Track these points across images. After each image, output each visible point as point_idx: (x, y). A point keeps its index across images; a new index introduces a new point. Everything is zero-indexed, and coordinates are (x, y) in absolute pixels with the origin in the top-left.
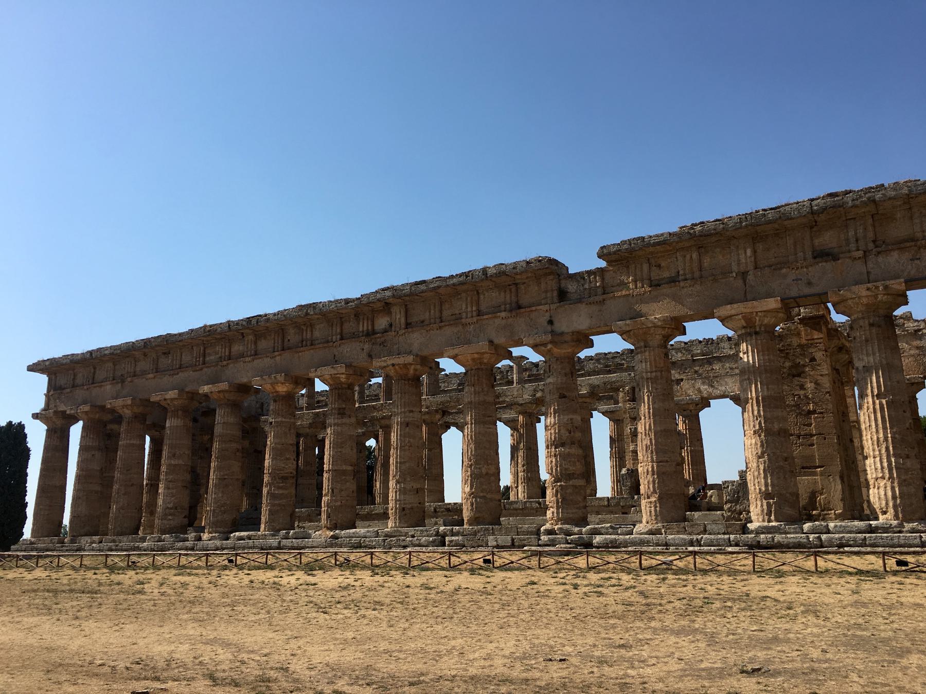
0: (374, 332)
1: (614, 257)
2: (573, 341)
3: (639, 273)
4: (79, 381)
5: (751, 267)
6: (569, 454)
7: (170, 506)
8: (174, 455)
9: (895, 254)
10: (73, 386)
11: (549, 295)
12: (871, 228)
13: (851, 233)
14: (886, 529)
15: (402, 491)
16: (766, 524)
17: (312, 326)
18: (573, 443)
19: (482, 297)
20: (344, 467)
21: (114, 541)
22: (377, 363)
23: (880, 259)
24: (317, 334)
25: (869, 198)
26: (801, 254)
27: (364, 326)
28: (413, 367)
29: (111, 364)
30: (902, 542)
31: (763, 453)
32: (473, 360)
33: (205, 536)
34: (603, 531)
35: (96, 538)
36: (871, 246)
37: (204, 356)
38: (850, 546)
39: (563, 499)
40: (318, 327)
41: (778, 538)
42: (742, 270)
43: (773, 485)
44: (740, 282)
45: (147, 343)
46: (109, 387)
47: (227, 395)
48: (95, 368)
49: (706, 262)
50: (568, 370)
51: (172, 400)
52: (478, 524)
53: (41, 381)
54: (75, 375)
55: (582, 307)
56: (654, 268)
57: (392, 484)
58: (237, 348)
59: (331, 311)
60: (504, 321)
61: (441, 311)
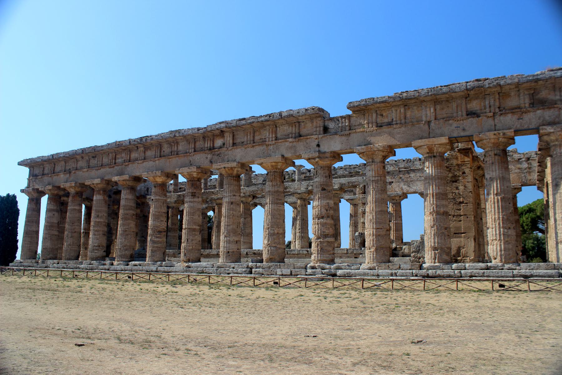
0: (214, 148)
1: (356, 109)
2: (331, 157)
3: (370, 119)
4: (46, 171)
5: (433, 118)
6: (326, 223)
7: (96, 245)
8: (98, 216)
9: (510, 116)
10: (43, 175)
11: (318, 129)
12: (498, 100)
13: (487, 103)
14: (495, 268)
15: (229, 242)
16: (433, 264)
17: (177, 143)
18: (328, 217)
19: (278, 129)
20: (194, 227)
21: (65, 263)
22: (215, 166)
23: (502, 118)
24: (180, 148)
25: (497, 83)
26: (460, 113)
27: (208, 144)
28: (236, 169)
29: (63, 163)
30: (503, 274)
31: (434, 225)
32: (272, 166)
33: (115, 263)
34: (343, 267)
35: (56, 261)
36: (497, 110)
37: (115, 159)
38: (476, 276)
39: (321, 249)
40: (181, 144)
41: (439, 272)
42: (428, 120)
43: (438, 243)
44: (427, 126)
45: (83, 150)
46: (62, 176)
48: (55, 165)
49: (409, 114)
50: (327, 174)
51: (97, 184)
53: (25, 171)
54: (44, 168)
55: (337, 137)
56: (379, 116)
57: (222, 237)
58: (134, 155)
59: (189, 135)
60: (291, 144)
61: (254, 137)
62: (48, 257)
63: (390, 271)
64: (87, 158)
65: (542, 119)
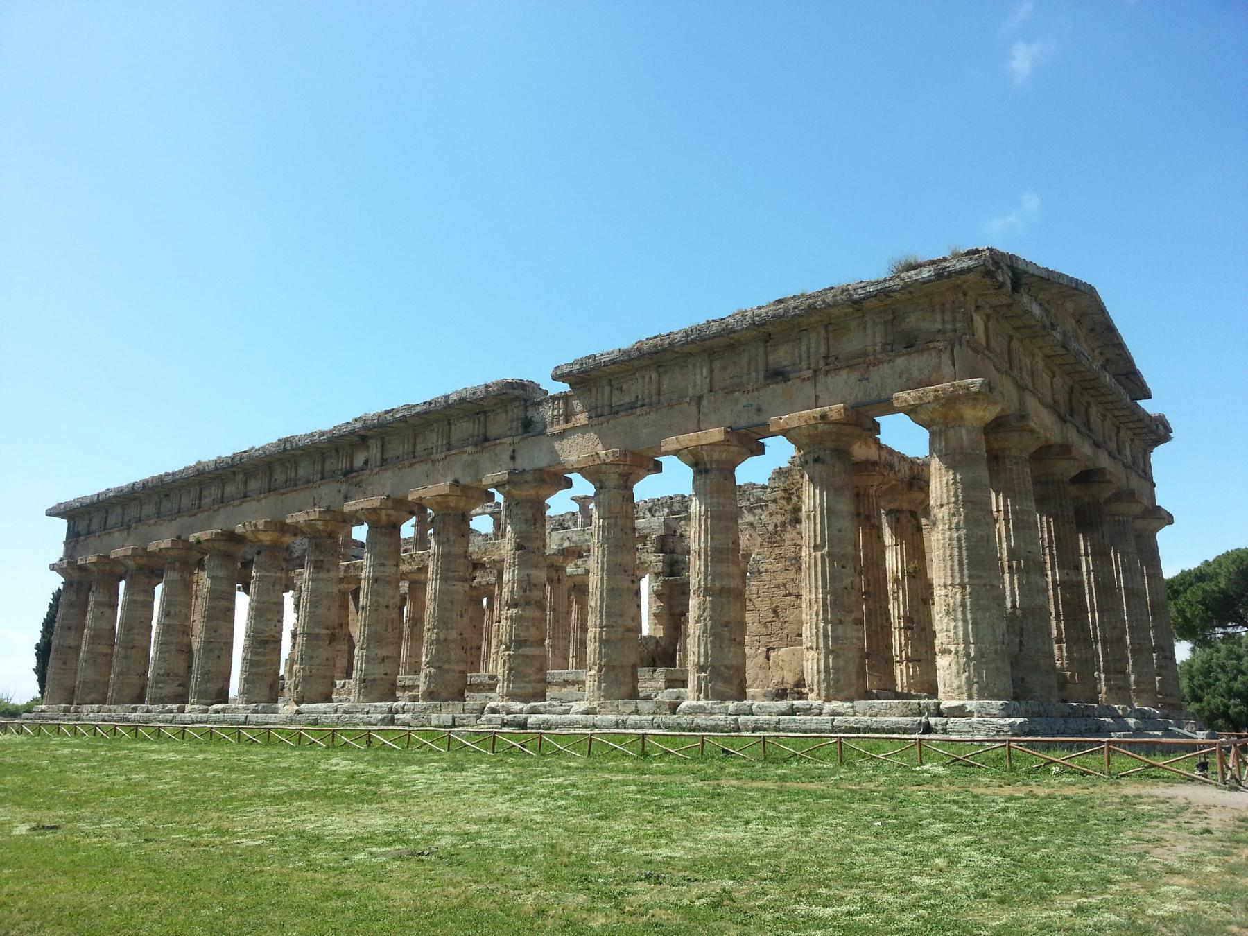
0: (352, 470)
2: (535, 480)
4: (94, 527)
5: (705, 390)
7: (162, 672)
9: (844, 373)
10: (89, 533)
13: (804, 348)
14: (807, 711)
15: (368, 660)
16: (695, 703)
17: (296, 464)
18: (528, 604)
20: (317, 630)
23: (829, 379)
24: (301, 472)
25: (809, 306)
27: (343, 464)
28: (384, 512)
29: (119, 510)
30: (814, 726)
31: (700, 616)
33: (188, 707)
34: (542, 709)
35: (95, 707)
36: (822, 363)
37: (200, 499)
38: (765, 730)
39: (511, 669)
41: (700, 720)
42: (697, 394)
46: (117, 534)
47: (216, 544)
49: (665, 384)
51: (167, 549)
52: (432, 699)
53: (62, 525)
54: (90, 521)
56: (615, 392)
58: (230, 489)
60: (471, 457)
61: (414, 445)
62: (88, 699)
63: (613, 717)
64: (156, 498)
65: (905, 376)
